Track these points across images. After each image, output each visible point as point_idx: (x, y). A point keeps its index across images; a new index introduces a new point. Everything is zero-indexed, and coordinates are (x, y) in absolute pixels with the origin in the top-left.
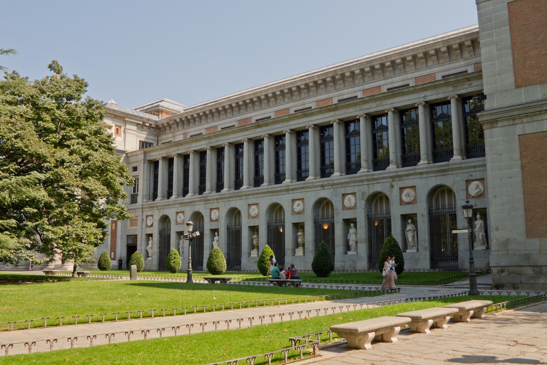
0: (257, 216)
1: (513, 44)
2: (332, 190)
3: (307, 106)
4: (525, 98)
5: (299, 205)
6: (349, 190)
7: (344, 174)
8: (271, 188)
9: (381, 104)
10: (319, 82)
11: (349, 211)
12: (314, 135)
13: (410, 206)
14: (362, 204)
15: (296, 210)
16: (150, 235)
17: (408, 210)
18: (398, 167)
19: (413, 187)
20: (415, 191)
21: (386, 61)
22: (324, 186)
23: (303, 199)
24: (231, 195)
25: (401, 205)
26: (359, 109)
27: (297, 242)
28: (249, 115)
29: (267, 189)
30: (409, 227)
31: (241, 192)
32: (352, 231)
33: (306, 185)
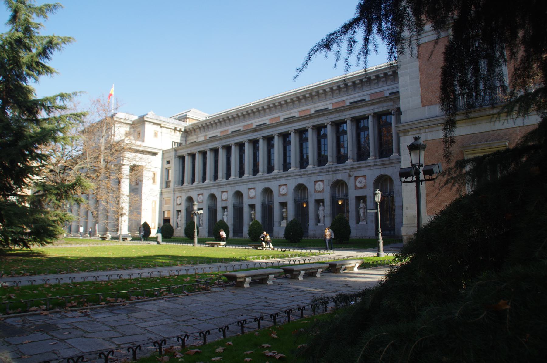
0: (254, 197)
1: (421, 74)
2: (307, 178)
3: (292, 115)
4: (428, 114)
5: (283, 189)
6: (319, 178)
7: (316, 166)
8: (265, 177)
9: (342, 114)
10: (301, 97)
11: (319, 194)
12: (295, 138)
13: (362, 190)
14: (328, 188)
15: (281, 193)
16: (179, 211)
17: (360, 193)
18: (354, 162)
19: (364, 176)
20: (366, 179)
21: (349, 81)
22: (301, 175)
23: (287, 185)
24: (236, 182)
25: (355, 189)
26: (327, 118)
27: (283, 216)
28: (250, 122)
29: (261, 177)
30: (362, 205)
31: (243, 179)
32: (321, 208)
33: (289, 175)
